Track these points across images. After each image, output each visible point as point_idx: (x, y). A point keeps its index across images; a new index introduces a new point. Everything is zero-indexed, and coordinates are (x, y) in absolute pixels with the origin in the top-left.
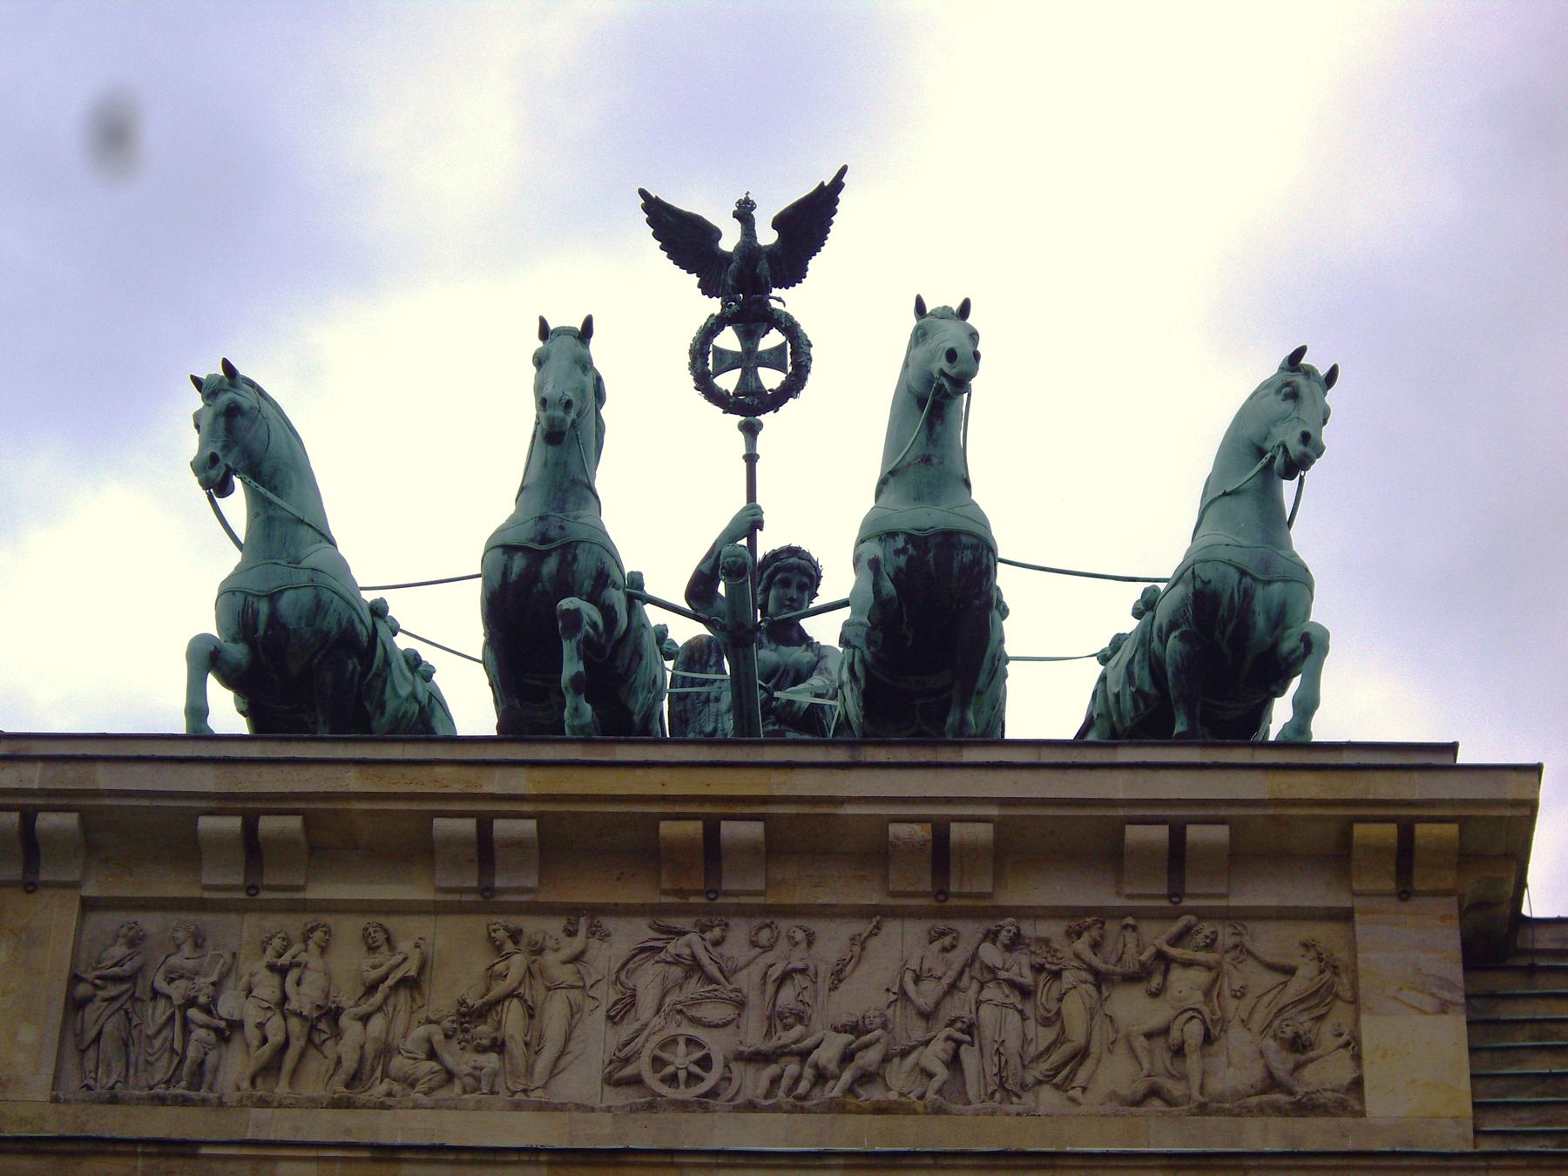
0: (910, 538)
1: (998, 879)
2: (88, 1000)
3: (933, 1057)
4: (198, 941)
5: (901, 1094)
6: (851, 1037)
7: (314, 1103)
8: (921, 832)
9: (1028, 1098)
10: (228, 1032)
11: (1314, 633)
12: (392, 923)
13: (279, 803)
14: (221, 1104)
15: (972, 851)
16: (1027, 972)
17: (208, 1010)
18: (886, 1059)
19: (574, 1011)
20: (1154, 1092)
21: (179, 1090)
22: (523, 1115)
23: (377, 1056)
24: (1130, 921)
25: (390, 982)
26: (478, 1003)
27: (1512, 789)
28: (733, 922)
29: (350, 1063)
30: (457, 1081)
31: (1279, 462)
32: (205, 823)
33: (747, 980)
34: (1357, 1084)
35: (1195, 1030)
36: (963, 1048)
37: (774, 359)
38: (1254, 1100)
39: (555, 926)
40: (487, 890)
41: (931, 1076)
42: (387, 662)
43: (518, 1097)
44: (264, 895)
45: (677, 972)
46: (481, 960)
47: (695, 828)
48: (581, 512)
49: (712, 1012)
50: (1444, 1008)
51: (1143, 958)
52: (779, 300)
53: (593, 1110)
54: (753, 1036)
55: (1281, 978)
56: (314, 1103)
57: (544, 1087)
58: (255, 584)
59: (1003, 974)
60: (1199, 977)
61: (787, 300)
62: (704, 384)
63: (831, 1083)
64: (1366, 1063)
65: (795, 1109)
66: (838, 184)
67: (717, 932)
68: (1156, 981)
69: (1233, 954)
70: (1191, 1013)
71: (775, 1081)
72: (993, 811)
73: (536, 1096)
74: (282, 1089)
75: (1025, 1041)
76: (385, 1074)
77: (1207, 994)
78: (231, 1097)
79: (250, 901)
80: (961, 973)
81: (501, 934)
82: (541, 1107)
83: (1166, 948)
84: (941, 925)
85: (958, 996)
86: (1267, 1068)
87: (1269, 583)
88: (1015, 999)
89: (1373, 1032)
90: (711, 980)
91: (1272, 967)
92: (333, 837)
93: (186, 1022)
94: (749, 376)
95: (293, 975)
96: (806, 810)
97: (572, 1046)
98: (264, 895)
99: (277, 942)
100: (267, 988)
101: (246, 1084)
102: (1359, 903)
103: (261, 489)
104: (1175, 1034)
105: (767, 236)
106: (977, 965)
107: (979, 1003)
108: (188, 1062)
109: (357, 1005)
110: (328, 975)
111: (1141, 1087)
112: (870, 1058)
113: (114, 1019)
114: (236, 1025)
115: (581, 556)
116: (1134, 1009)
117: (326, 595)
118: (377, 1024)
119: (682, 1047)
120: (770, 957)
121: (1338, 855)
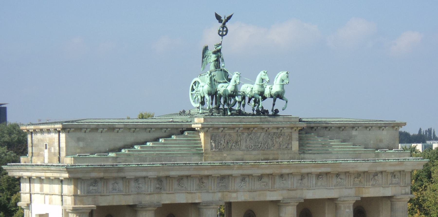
13: (226, 128)
39: (241, 134)
58: (209, 90)
89: (293, 142)
94: (223, 33)
100: (223, 141)
105: (226, 18)
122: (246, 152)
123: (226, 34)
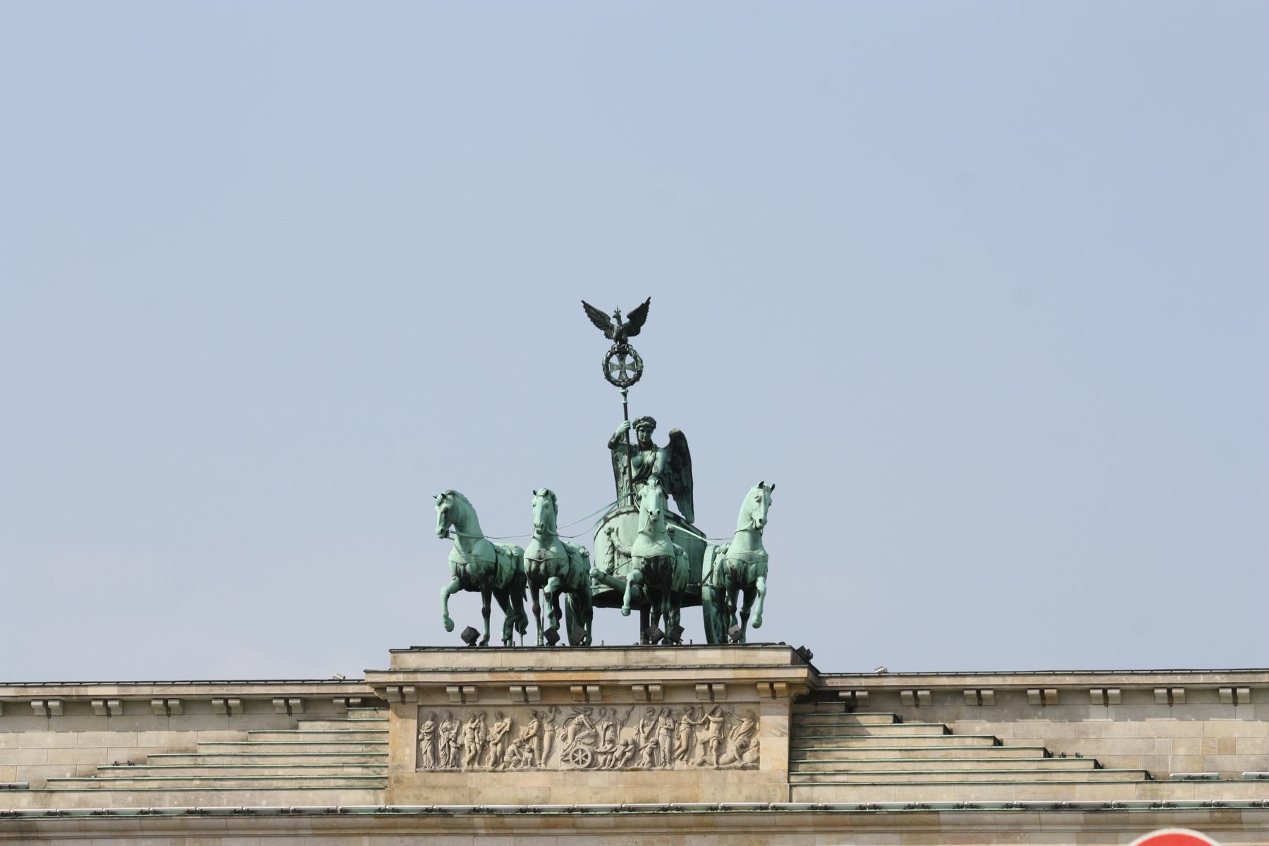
3: (645, 754)
10: (460, 748)
12: (503, 710)
17: (455, 742)
19: (552, 739)
21: (448, 768)
29: (492, 759)
35: (715, 743)
37: (632, 366)
39: (546, 709)
40: (526, 700)
49: (588, 741)
62: (608, 377)
66: (648, 302)
73: (543, 766)
74: (476, 766)
75: (671, 745)
78: (463, 769)
92: (482, 689)
94: (623, 372)
105: (625, 320)
112: (628, 754)
116: (702, 735)
118: (499, 746)
123: (637, 378)
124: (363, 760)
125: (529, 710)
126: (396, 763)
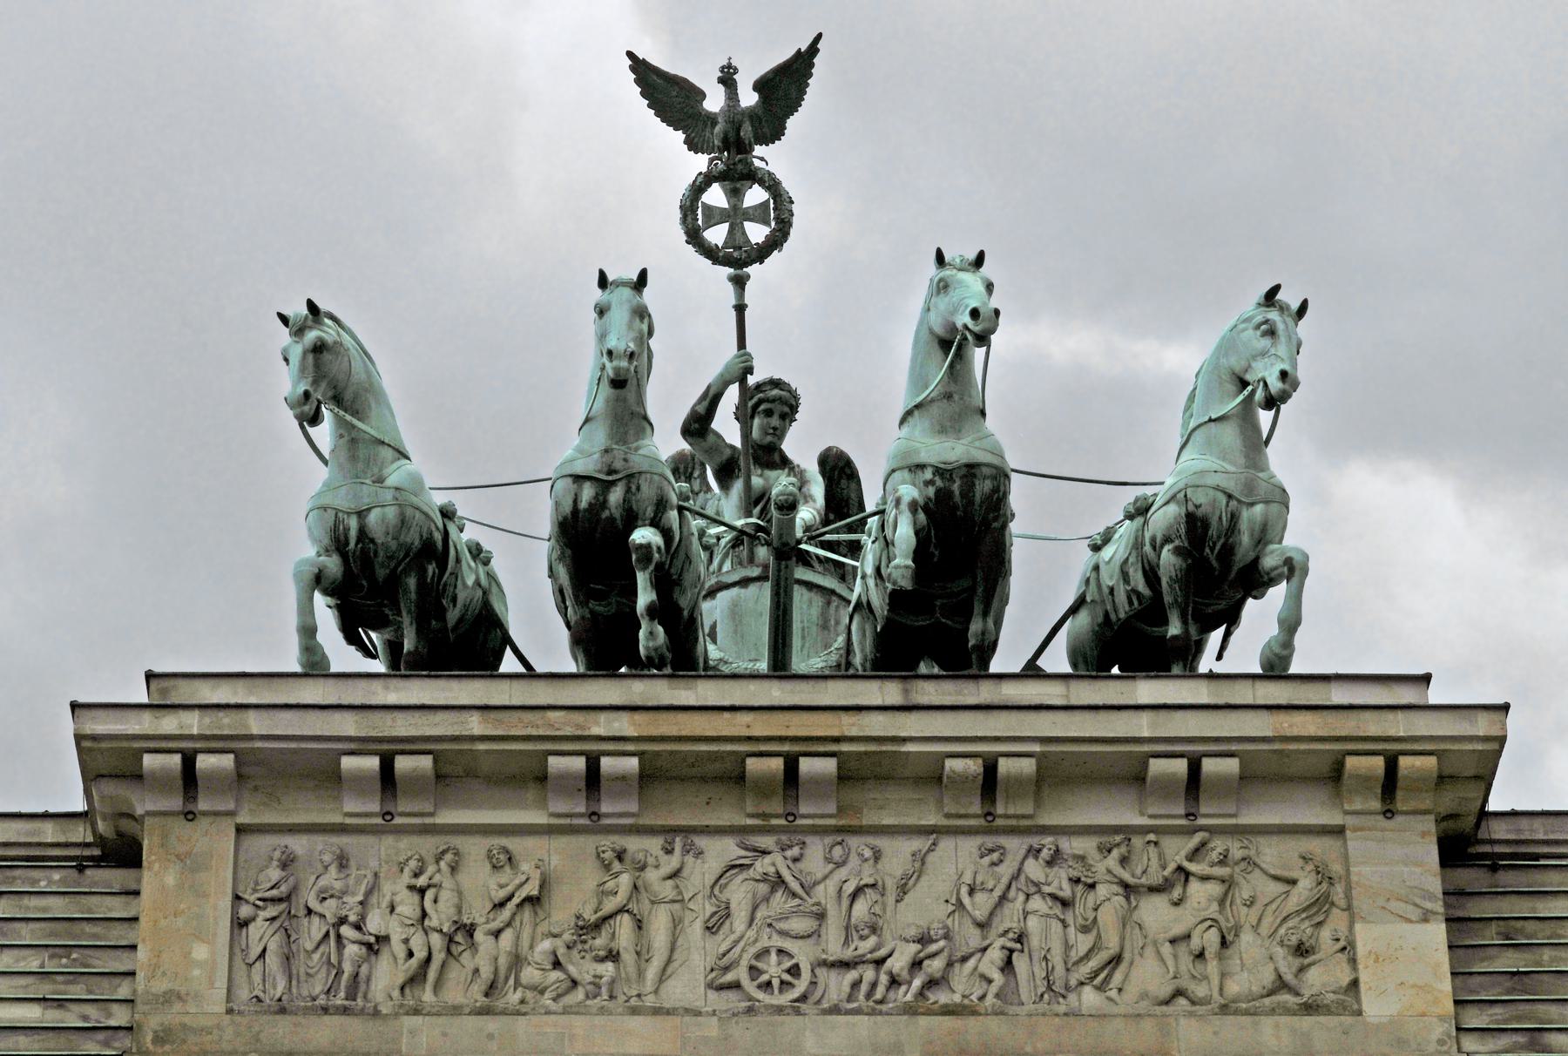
0: (938, 471)
1: (1038, 802)
2: (254, 919)
4: (342, 862)
5: (964, 996)
6: (915, 947)
7: (456, 1010)
8: (974, 767)
9: (1072, 997)
10: (375, 945)
11: (1297, 557)
12: (513, 843)
14: (376, 1013)
15: (1018, 782)
16: (1066, 885)
17: (358, 927)
18: (950, 964)
19: (676, 923)
20: (1179, 992)
21: (340, 1000)
22: (640, 1018)
23: (509, 969)
24: (1152, 837)
25: (516, 900)
26: (593, 918)
27: (1483, 726)
28: (809, 839)
29: (486, 973)
30: (580, 988)
31: (1260, 395)
32: (348, 763)
33: (824, 894)
34: (1355, 983)
35: (1213, 937)
36: (1015, 955)
38: (1267, 1001)
39: (654, 844)
40: (594, 815)
41: (990, 981)
42: (458, 560)
43: (633, 1001)
44: (398, 820)
45: (763, 888)
46: (591, 876)
47: (777, 764)
48: (640, 442)
49: (799, 925)
50: (1426, 920)
51: (1166, 873)
52: (762, 159)
53: (698, 1013)
54: (834, 947)
55: (1281, 887)
56: (456, 1010)
57: (656, 992)
58: (342, 501)
59: (1047, 889)
60: (1215, 889)
61: (767, 156)
63: (903, 988)
64: (1361, 967)
65: (873, 1012)
66: (813, 49)
67: (795, 851)
68: (1176, 893)
69: (1243, 865)
70: (1209, 923)
71: (856, 985)
72: (1037, 748)
73: (650, 1001)
74: (428, 996)
75: (1067, 947)
76: (517, 984)
77: (1222, 902)
79: (386, 825)
80: (1009, 887)
81: (608, 855)
82: (657, 1011)
83: (1186, 864)
84: (990, 841)
85: (1008, 909)
86: (1276, 969)
87: (1252, 504)
88: (1058, 910)
89: (1366, 937)
90: (794, 895)
91: (1276, 878)
92: (456, 770)
93: (339, 937)
95: (429, 895)
96: (872, 748)
97: (676, 956)
98: (398, 820)
99: (413, 864)
100: (408, 906)
101: (396, 994)
102: (1350, 821)
103: (348, 417)
104: (1195, 943)
105: (748, 98)
106: (1022, 878)
107: (1026, 914)
108: (346, 976)
109: (487, 922)
110: (460, 893)
111: (1166, 990)
112: (935, 966)
113: (277, 937)
114: (383, 939)
115: (644, 487)
116: (1156, 913)
117: (409, 512)
118: (507, 936)
119: (774, 957)
120: (842, 873)
121: (1334, 775)
122: (711, 1028)
124: (45, 989)
125: (608, 842)
126: (160, 986)
